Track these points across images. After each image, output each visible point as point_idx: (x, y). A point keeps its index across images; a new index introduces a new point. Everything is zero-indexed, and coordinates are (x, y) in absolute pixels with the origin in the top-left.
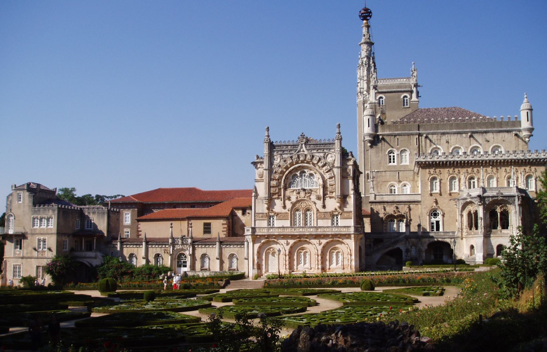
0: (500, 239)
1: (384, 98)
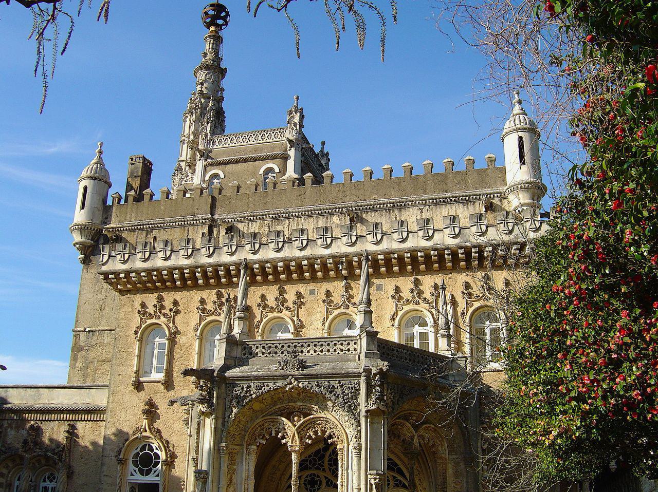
1: (222, 176)
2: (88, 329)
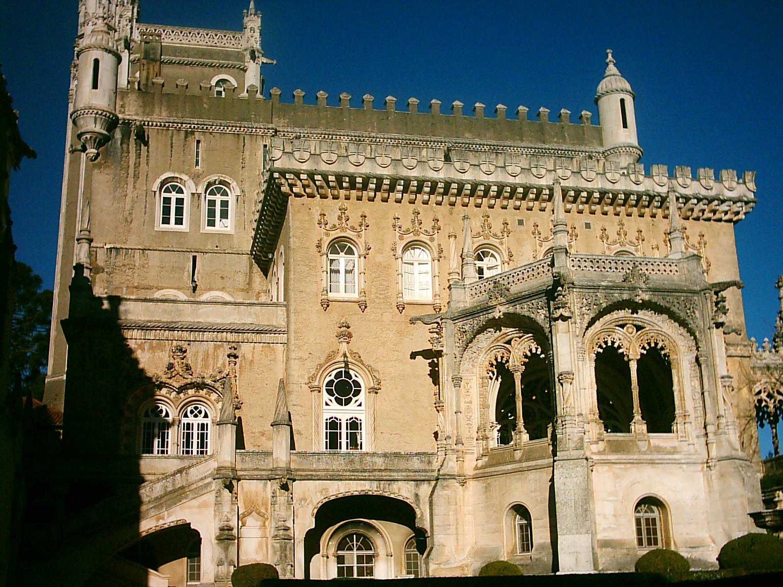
0: (648, 472)
2: (108, 246)
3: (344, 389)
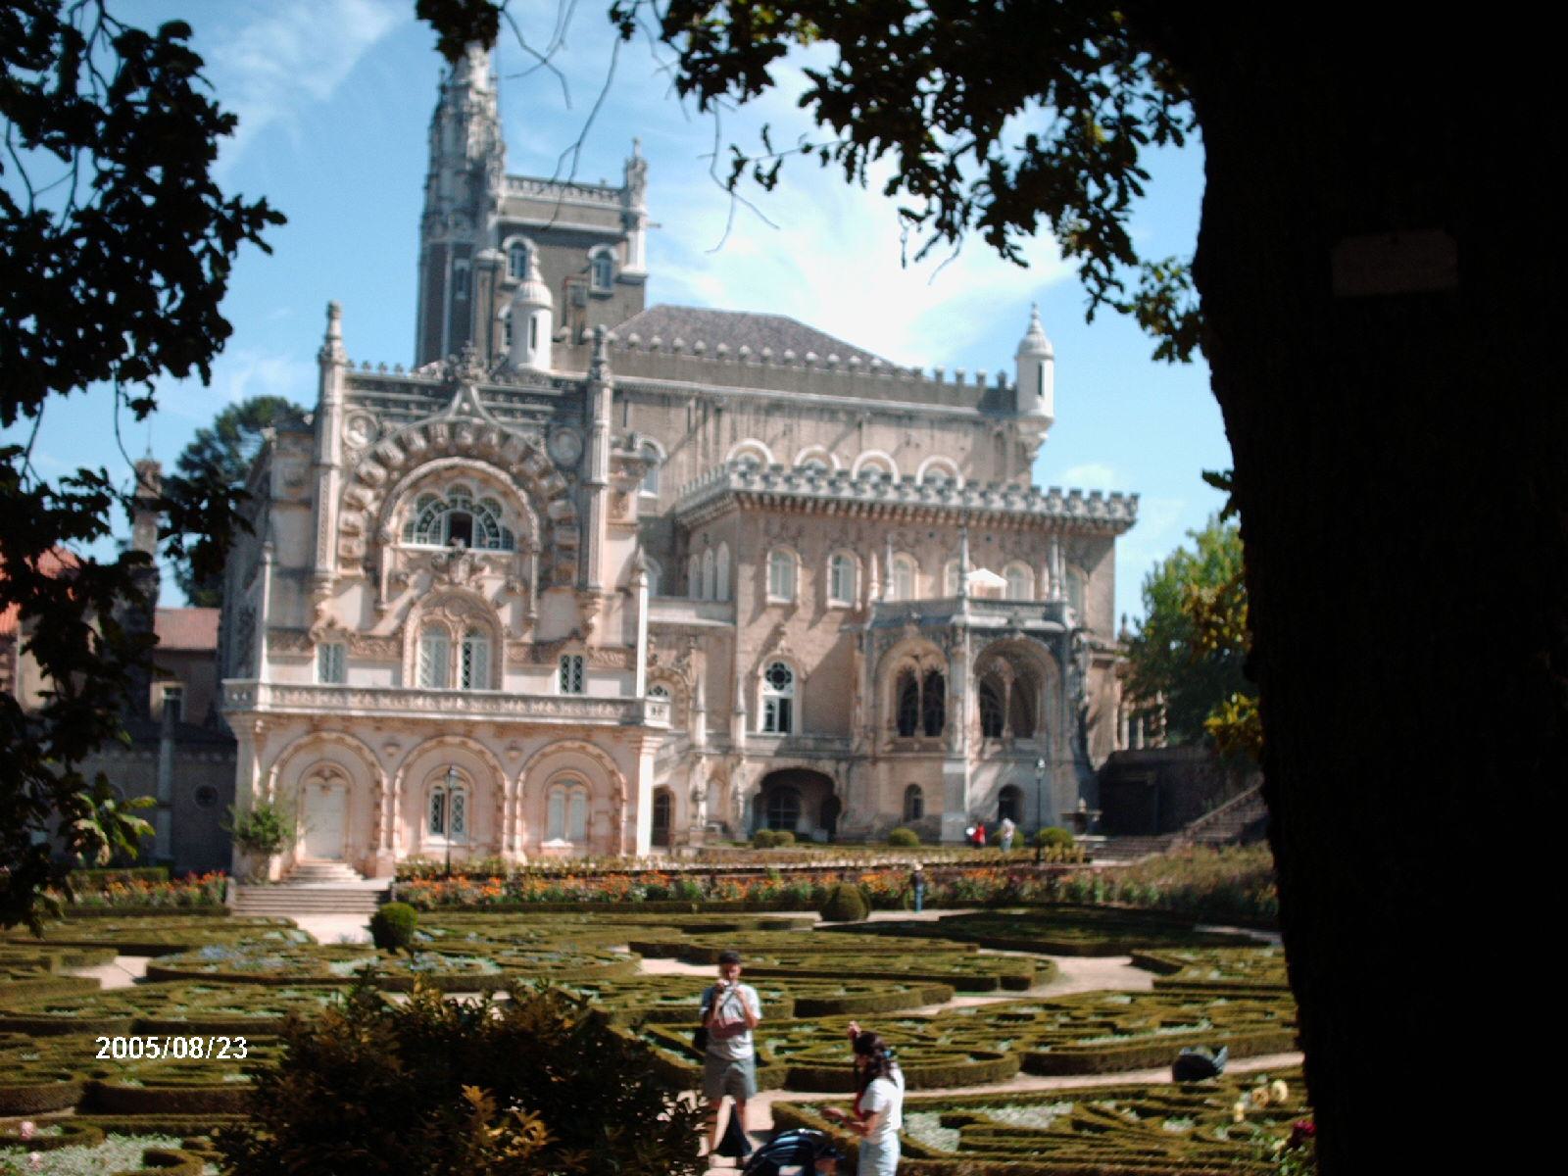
3: (779, 676)
